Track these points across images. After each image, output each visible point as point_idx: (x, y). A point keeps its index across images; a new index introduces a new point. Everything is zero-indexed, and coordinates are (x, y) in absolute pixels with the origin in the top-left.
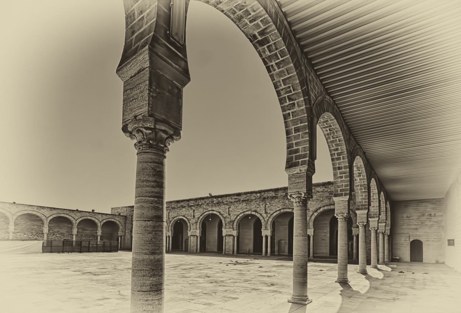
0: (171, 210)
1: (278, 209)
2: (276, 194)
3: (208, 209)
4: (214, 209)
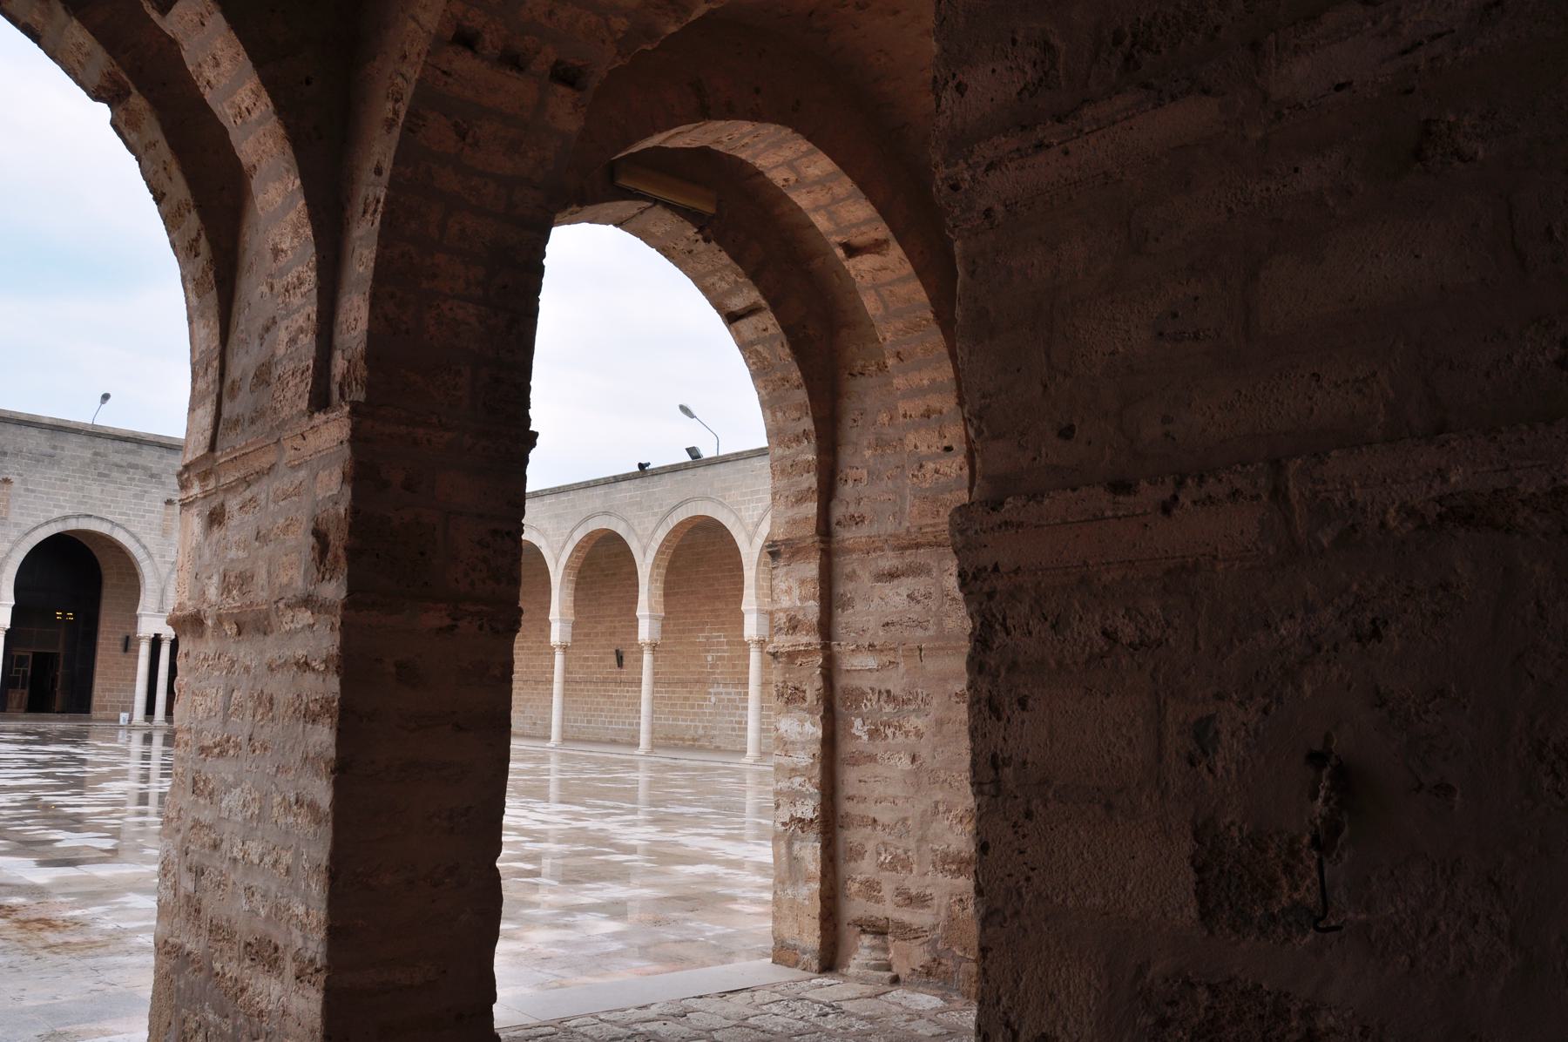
1: (56, 513)
2: (55, 447)
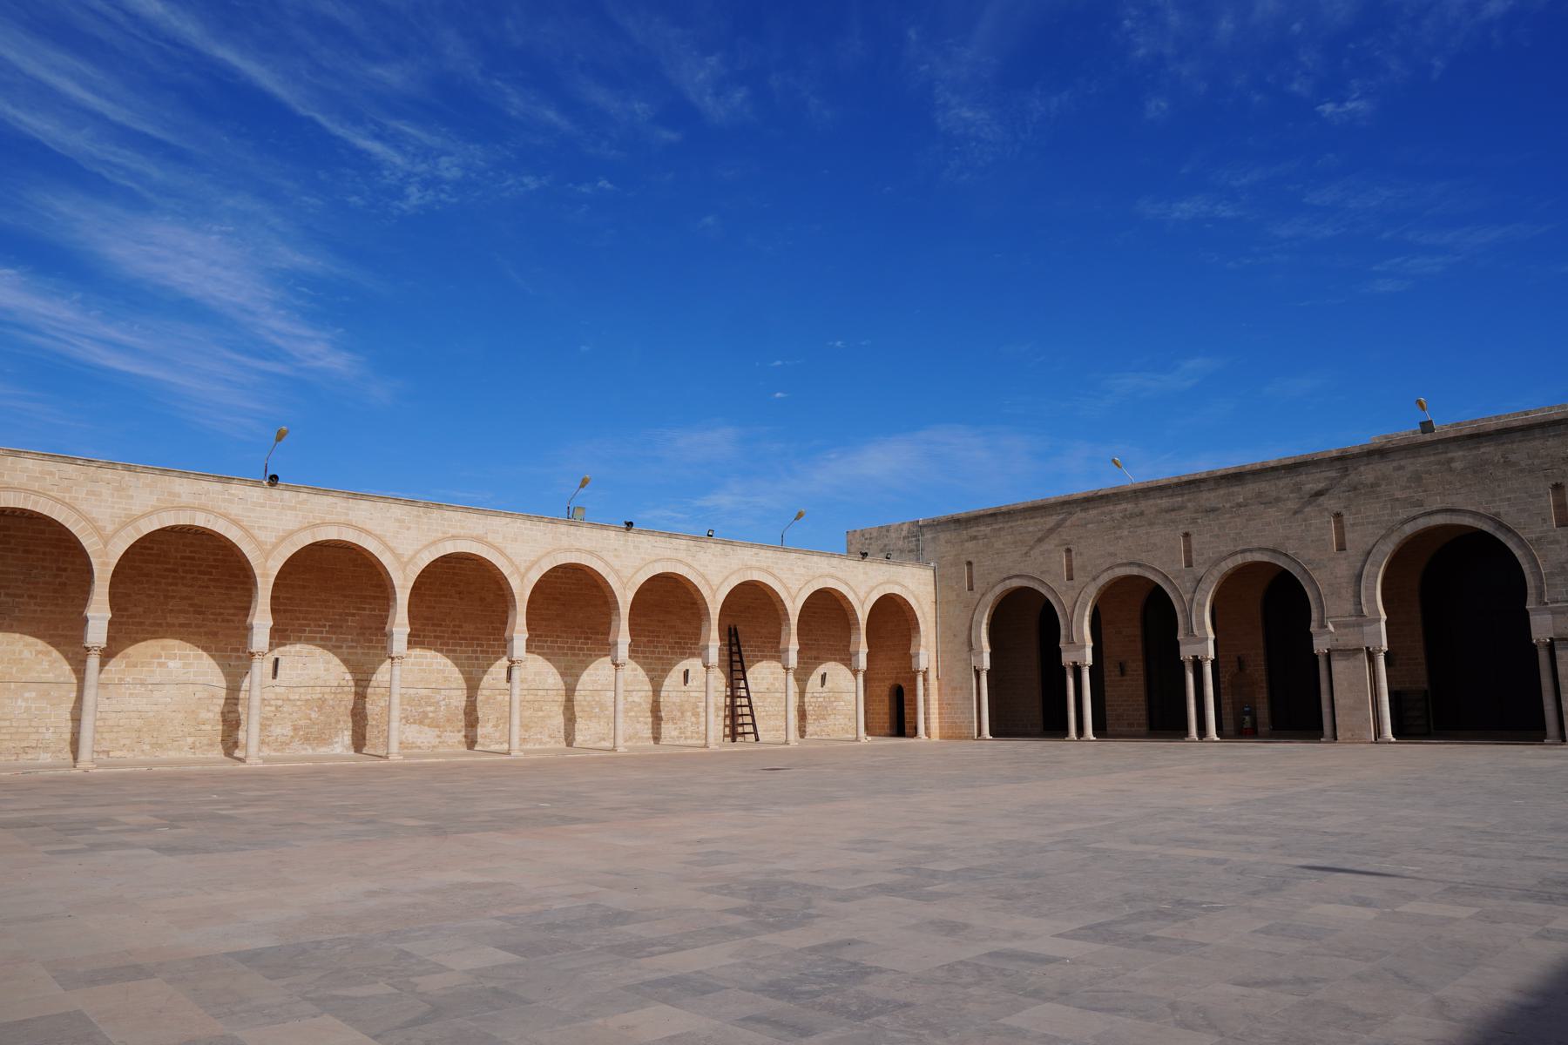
0: (1194, 521)
3: (1420, 504)
4: (1458, 501)
